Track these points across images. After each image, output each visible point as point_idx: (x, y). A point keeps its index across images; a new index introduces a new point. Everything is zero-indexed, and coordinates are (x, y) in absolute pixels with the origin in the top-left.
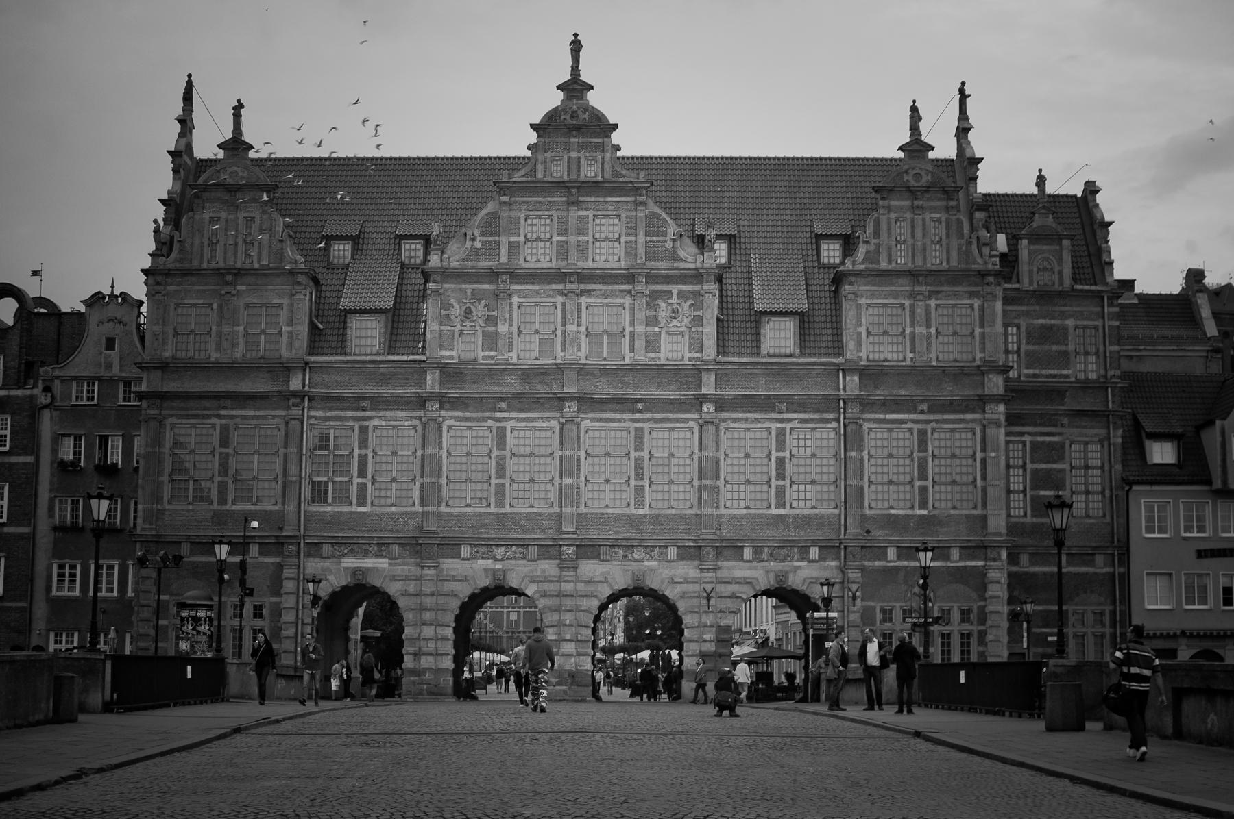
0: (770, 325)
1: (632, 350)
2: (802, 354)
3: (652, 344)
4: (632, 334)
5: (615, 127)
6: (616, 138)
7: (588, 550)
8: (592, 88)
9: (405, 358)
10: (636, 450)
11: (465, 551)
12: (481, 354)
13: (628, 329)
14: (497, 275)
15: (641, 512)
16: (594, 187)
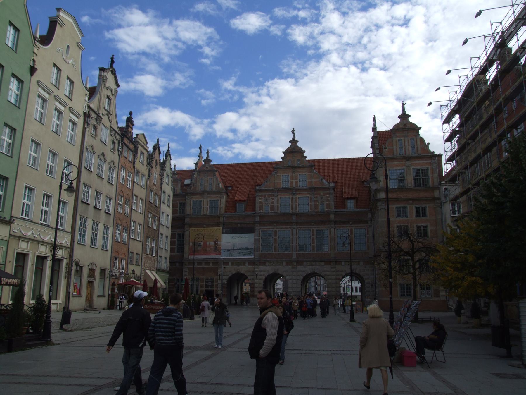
0: (348, 201)
1: (311, 209)
2: (357, 209)
3: (316, 206)
4: (311, 205)
5: (305, 151)
6: (305, 154)
7: (299, 262)
8: (298, 142)
9: (251, 213)
10: (313, 236)
11: (267, 264)
12: (270, 211)
13: (309, 204)
14: (274, 191)
15: (314, 252)
16: (299, 167)
